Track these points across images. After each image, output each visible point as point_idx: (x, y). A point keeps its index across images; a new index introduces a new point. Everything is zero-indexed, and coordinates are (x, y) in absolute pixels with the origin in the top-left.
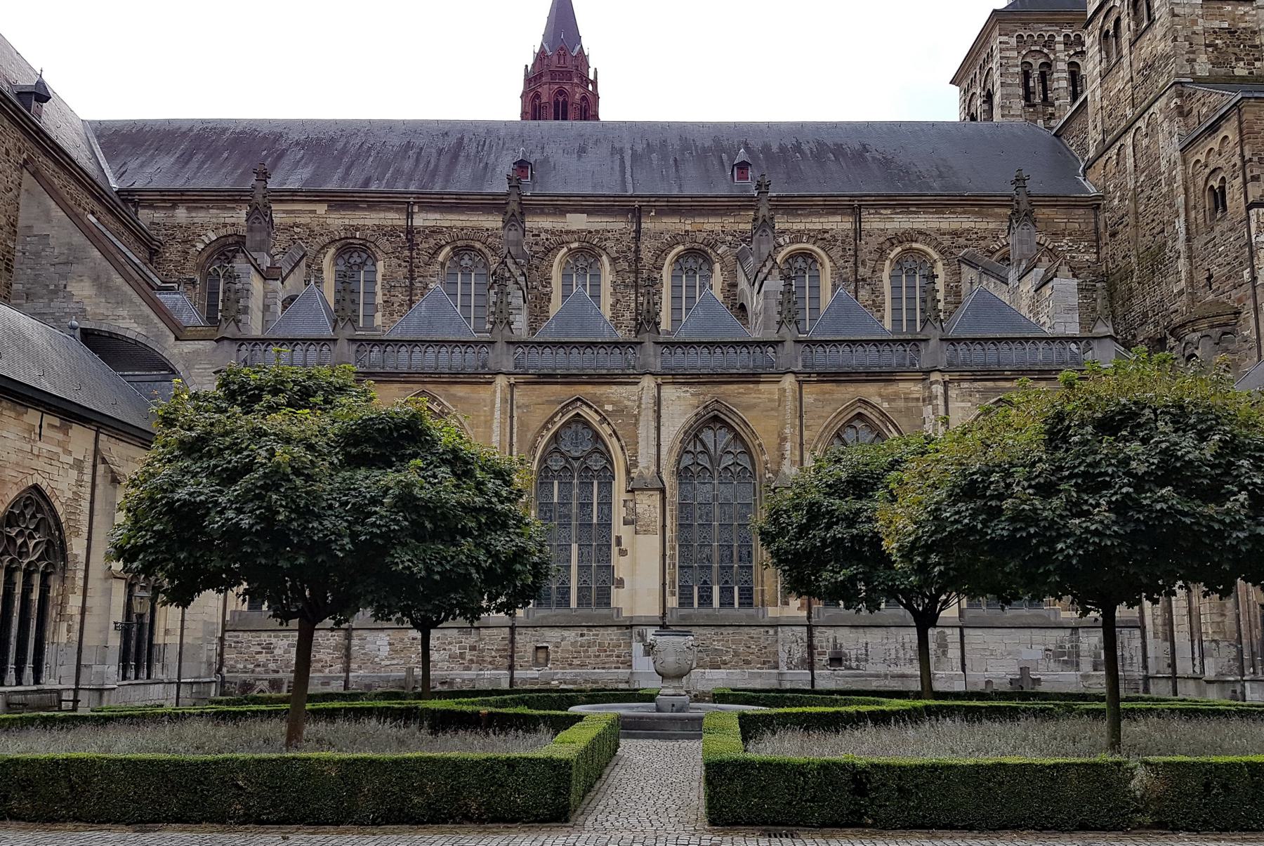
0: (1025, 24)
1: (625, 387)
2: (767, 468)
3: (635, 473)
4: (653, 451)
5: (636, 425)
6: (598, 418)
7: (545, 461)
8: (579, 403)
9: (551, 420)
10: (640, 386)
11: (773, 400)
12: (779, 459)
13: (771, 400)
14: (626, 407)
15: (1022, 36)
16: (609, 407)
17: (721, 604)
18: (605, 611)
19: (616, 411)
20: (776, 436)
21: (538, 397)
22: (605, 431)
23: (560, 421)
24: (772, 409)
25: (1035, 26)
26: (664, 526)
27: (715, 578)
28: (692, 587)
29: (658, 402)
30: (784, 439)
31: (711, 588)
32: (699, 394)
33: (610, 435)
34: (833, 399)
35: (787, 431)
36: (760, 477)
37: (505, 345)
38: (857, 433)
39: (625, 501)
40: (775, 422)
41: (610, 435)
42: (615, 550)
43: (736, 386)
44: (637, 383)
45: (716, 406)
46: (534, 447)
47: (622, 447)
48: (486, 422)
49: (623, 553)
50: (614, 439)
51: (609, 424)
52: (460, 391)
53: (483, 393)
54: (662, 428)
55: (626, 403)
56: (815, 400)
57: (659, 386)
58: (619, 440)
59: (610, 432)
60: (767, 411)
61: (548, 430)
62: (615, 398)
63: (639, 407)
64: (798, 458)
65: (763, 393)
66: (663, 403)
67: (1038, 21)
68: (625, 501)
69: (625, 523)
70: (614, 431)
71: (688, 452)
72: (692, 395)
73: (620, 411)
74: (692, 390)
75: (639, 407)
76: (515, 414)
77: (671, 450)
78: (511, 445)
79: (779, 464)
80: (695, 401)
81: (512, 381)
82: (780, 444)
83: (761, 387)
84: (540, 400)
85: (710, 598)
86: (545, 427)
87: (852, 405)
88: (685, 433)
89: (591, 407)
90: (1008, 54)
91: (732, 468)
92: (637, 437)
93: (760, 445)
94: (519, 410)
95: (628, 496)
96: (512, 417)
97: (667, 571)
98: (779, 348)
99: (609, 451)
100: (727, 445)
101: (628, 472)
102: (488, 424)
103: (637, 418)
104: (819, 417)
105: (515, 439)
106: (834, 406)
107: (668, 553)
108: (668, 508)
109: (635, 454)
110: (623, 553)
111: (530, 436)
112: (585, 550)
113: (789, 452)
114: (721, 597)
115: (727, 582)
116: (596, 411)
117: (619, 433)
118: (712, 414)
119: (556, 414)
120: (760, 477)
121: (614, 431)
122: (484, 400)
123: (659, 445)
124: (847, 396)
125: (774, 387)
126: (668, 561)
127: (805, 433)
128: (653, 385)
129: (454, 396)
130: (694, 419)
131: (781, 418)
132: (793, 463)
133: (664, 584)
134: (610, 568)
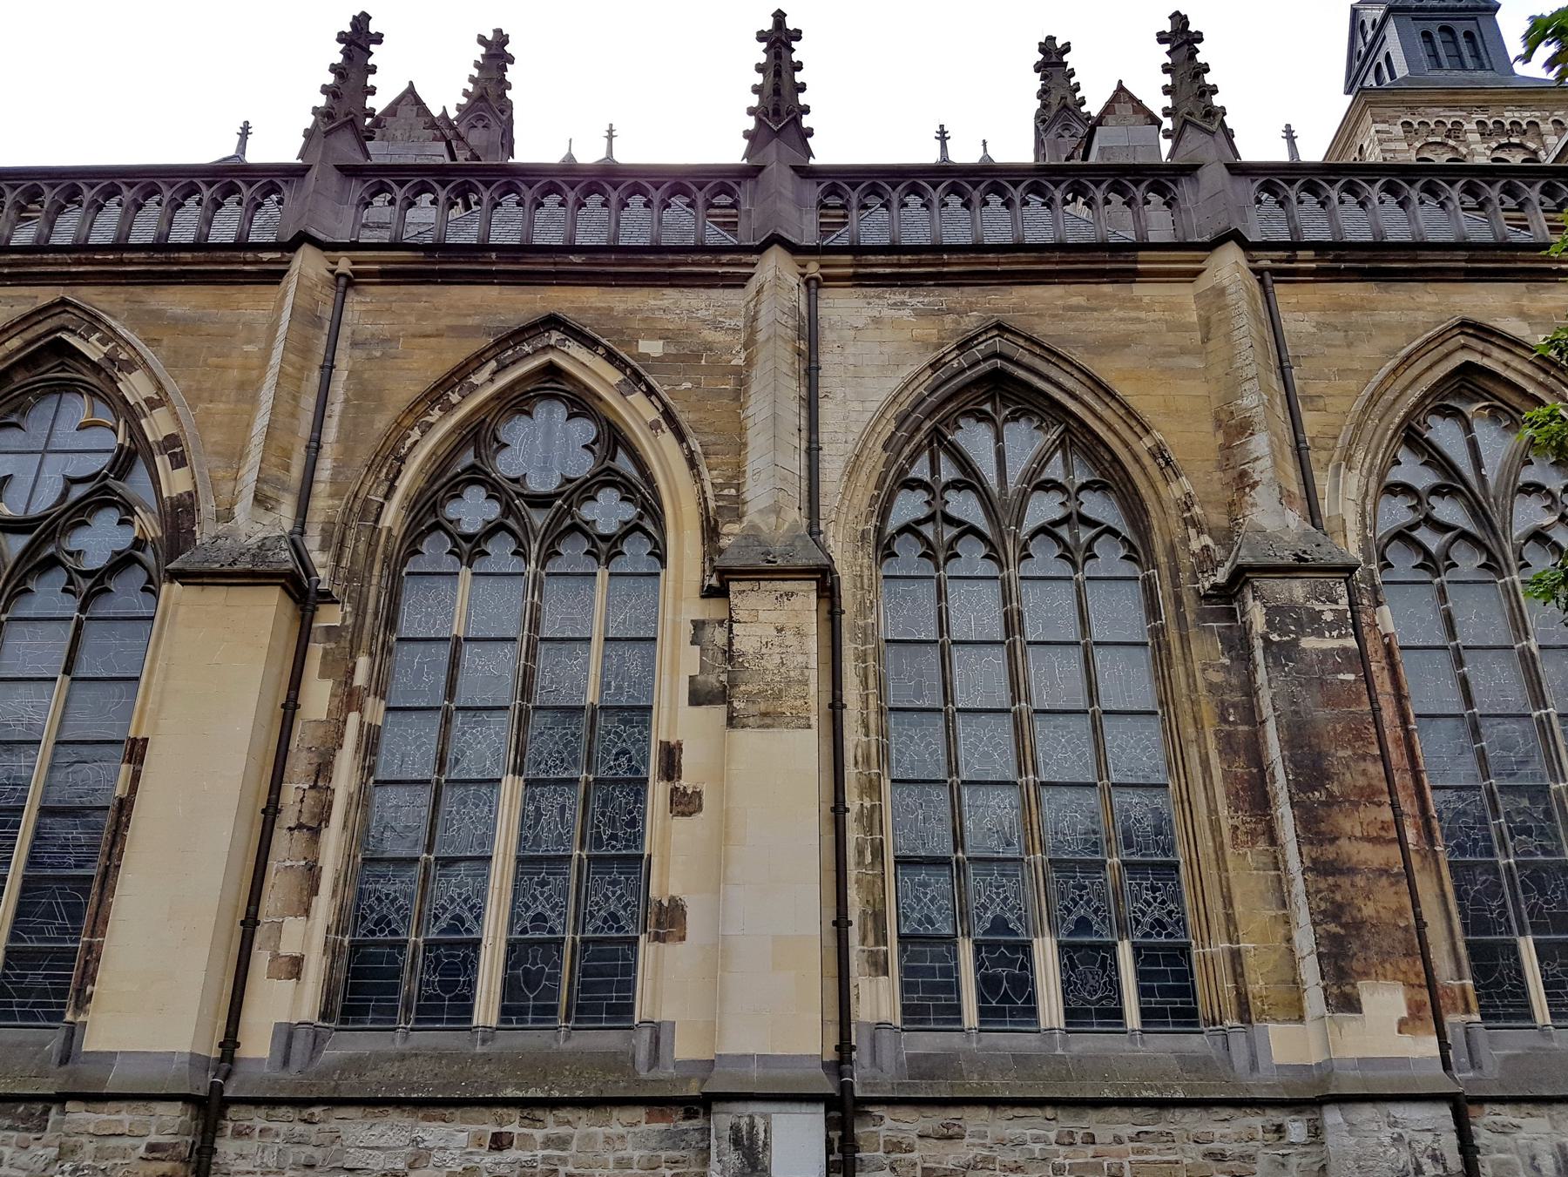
0: (1412, 109)
1: (704, 293)
2: (1192, 522)
3: (731, 531)
4: (796, 463)
5: (739, 394)
6: (614, 376)
7: (435, 507)
8: (555, 336)
9: (458, 376)
10: (752, 285)
11: (1185, 327)
12: (1229, 495)
13: (1179, 327)
14: (709, 347)
15: (1410, 124)
16: (652, 347)
17: (1071, 1014)
18: (607, 1040)
19: (677, 357)
20: (1209, 426)
21: (422, 316)
22: (636, 413)
23: (487, 385)
24: (1184, 351)
25: (1428, 110)
26: (836, 707)
27: (1038, 906)
28: (951, 941)
29: (809, 335)
30: (1236, 429)
31: (1026, 948)
32: (941, 312)
33: (654, 426)
34: (1375, 325)
35: (1250, 401)
36: (1172, 551)
37: (334, 177)
38: (1468, 428)
39: (698, 625)
40: (1197, 388)
41: (654, 426)
42: (658, 792)
43: (1057, 290)
44: (739, 282)
45: (999, 344)
46: (391, 457)
47: (692, 463)
48: (242, 386)
49: (685, 804)
50: (667, 438)
51: (650, 391)
52: (176, 301)
53: (249, 304)
54: (826, 409)
55: (709, 335)
56: (1320, 326)
57: (813, 285)
58: (681, 436)
59: (652, 414)
60: (1170, 355)
61: (449, 408)
62: (672, 322)
63: (749, 344)
64: (1295, 488)
65: (1149, 308)
66: (828, 338)
67: (1432, 104)
68: (698, 625)
69: (698, 697)
70: (668, 415)
71: (914, 484)
72: (919, 314)
73: (687, 357)
74: (921, 298)
75: (749, 344)
76: (343, 363)
77: (853, 469)
78: (314, 448)
79: (1233, 508)
80: (929, 331)
81: (344, 266)
82: (1226, 447)
83: (1141, 290)
84: (428, 326)
85: (1024, 986)
86: (437, 394)
87: (1441, 338)
88: (902, 420)
89: (590, 343)
90: (1393, 146)
91: (1064, 532)
92: (742, 430)
93: (1159, 452)
94: (357, 353)
95: (711, 610)
96: (328, 368)
97: (852, 873)
98: (1184, 189)
99: (649, 480)
100: (1043, 461)
101: (711, 532)
102: (247, 390)
103: (741, 379)
104: (1343, 373)
105: (331, 432)
106: (1385, 341)
107: (853, 801)
108: (849, 649)
109: (736, 478)
110: (685, 804)
111: (382, 422)
112: (550, 800)
113: (1266, 463)
114: (1067, 987)
115: (1083, 925)
116: (611, 357)
117: (683, 418)
118: (985, 367)
119: (477, 361)
120: (1172, 551)
121: (668, 415)
122: (249, 326)
123: (813, 452)
124: (1421, 316)
125: (1183, 293)
126: (853, 834)
127: (1309, 419)
128: (793, 280)
129: (157, 315)
130: (928, 379)
131: (1219, 371)
132: (1285, 497)
133: (841, 924)
134: (635, 864)
